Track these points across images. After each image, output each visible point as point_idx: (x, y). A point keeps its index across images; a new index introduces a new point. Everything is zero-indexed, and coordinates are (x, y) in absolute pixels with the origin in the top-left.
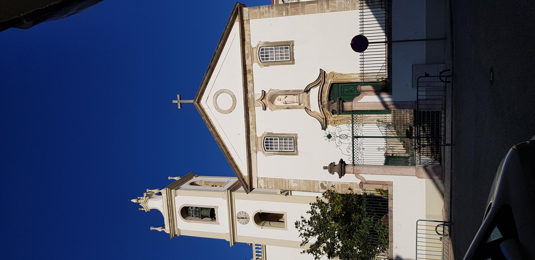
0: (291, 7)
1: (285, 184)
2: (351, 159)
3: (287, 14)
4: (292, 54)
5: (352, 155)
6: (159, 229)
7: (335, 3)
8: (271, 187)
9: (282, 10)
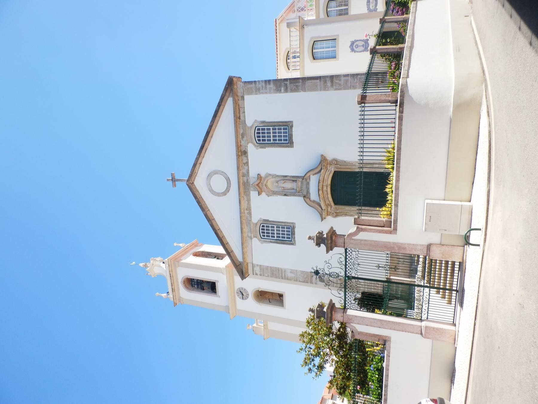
0: (290, 83)
1: (282, 274)
2: (343, 302)
3: (286, 91)
4: (291, 136)
5: (343, 298)
6: (164, 295)
7: (340, 80)
9: (280, 86)
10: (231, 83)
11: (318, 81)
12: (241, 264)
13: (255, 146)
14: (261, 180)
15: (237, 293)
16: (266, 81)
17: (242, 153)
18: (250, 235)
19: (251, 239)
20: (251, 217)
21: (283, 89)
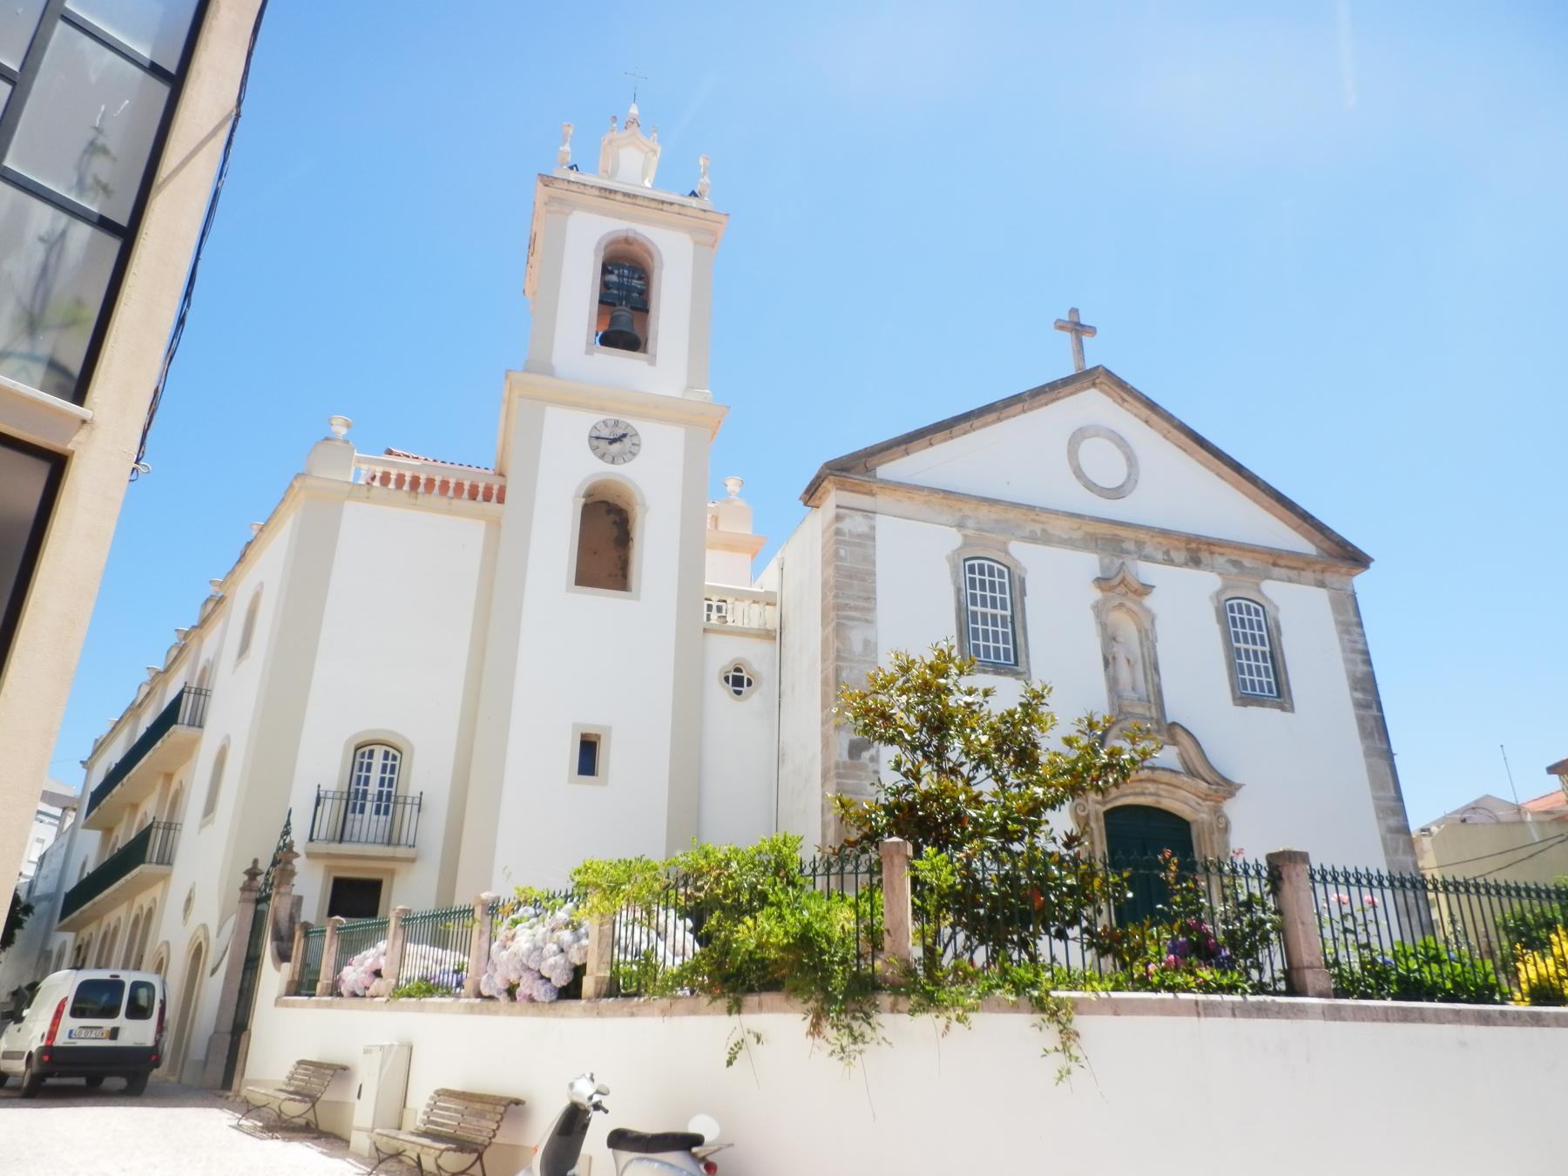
0: (1375, 717)
1: (856, 608)
8: (842, 552)
9: (1364, 690)
10: (1357, 559)
11: (1393, 793)
12: (869, 471)
13: (1218, 594)
14: (1135, 592)
15: (616, 423)
16: (1366, 653)
17: (1196, 550)
18: (970, 523)
19: (960, 526)
20: (1024, 539)
21: (1359, 695)
